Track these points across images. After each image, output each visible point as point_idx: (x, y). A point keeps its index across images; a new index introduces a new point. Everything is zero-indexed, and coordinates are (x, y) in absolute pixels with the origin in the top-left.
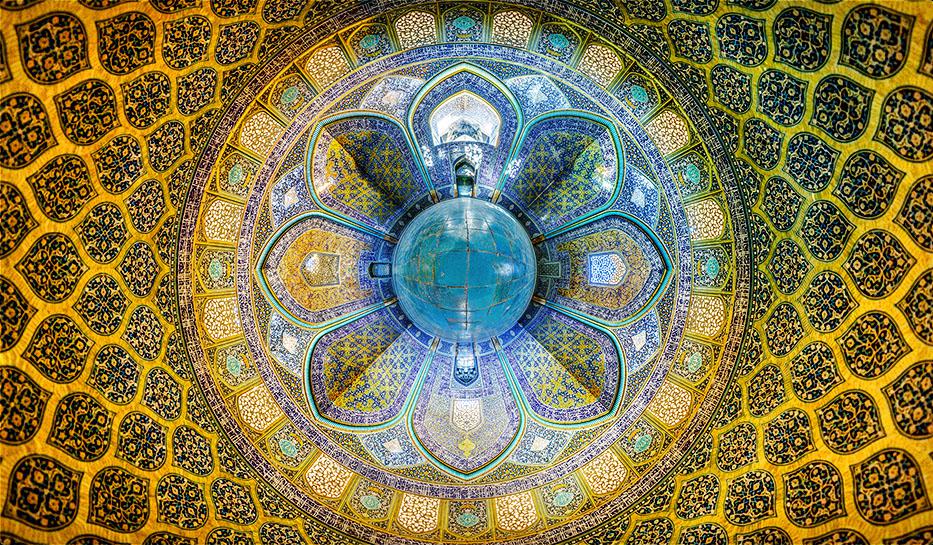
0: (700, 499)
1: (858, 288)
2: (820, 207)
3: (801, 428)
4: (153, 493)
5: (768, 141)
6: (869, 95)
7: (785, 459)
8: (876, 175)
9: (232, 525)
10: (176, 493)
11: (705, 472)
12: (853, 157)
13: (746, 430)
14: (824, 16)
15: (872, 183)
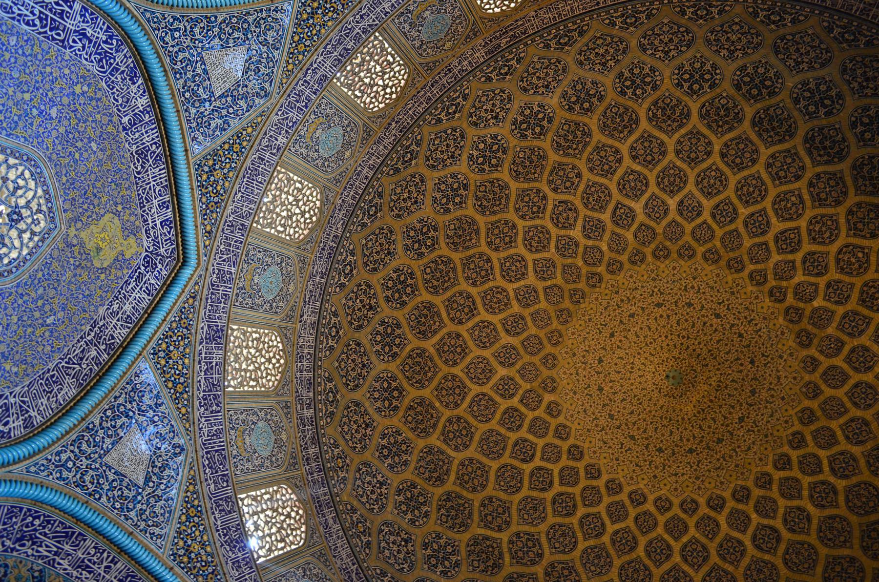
0: (492, 111)
1: (707, 101)
2: (779, 86)
3: (595, 99)
4: (464, 562)
5: (865, 84)
6: (815, 163)
7: (571, 109)
8: (777, 134)
9: (405, 526)
10: (446, 562)
11: (504, 85)
12: (796, 128)
13: (560, 67)
14: (861, 194)
15: (773, 129)
